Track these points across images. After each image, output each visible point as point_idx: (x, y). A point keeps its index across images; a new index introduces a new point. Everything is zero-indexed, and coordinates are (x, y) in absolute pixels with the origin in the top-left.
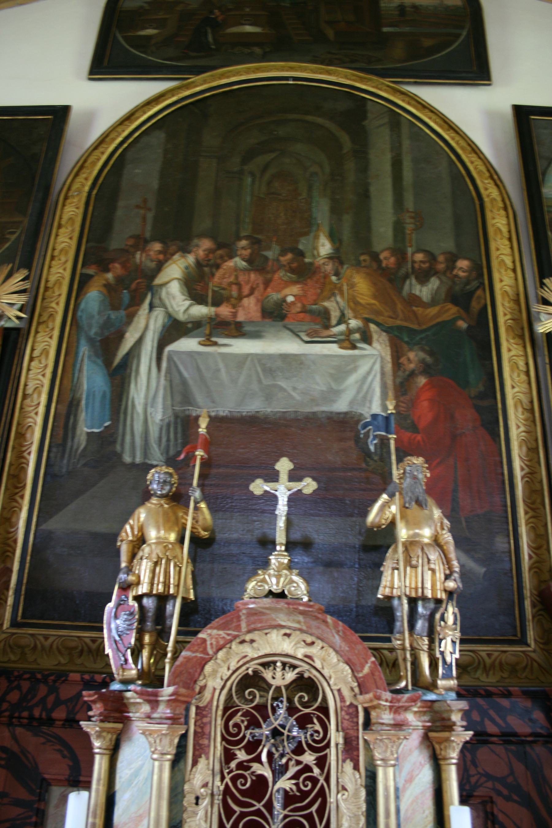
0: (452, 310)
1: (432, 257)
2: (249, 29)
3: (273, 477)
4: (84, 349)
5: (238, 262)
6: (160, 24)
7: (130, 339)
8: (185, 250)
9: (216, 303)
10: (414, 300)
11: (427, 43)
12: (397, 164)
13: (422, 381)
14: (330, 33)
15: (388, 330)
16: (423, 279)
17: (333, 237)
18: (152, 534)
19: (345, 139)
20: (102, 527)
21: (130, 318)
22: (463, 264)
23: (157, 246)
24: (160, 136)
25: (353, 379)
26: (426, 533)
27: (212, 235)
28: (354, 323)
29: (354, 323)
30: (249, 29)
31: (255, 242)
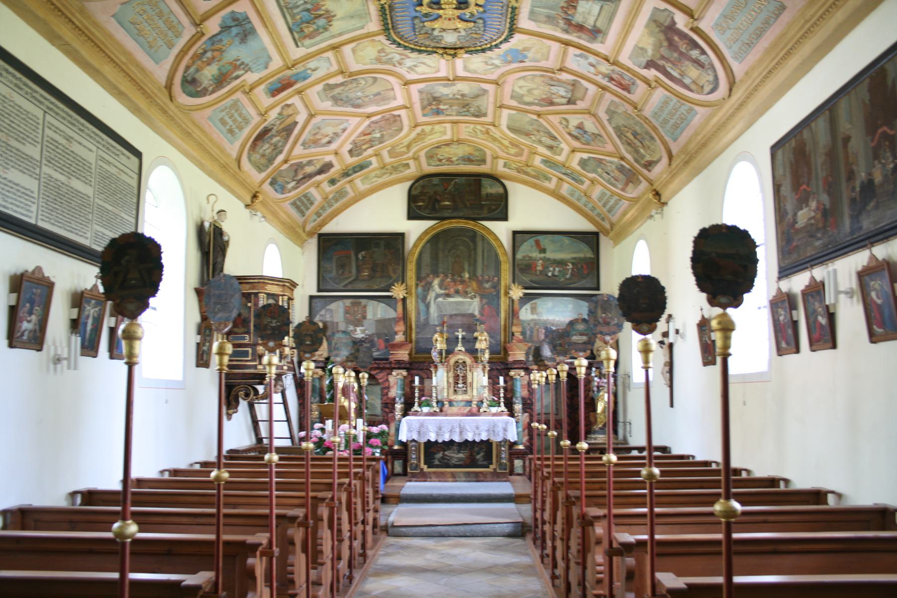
0: (493, 290)
1: (489, 277)
2: (447, 203)
3: (458, 332)
4: (420, 301)
5: (449, 280)
6: (423, 201)
7: (429, 298)
8: (438, 277)
9: (446, 289)
10: (485, 288)
11: (494, 207)
12: (483, 252)
13: (486, 306)
14: (468, 204)
15: (479, 295)
16: (487, 282)
17: (469, 273)
18: (439, 339)
19: (471, 245)
20: (429, 336)
21: (428, 294)
22: (496, 278)
23: (431, 276)
24: (429, 244)
25: (472, 306)
26: (484, 338)
27: (443, 273)
28: (473, 294)
29: (473, 294)
30: (447, 203)
31: (453, 275)
